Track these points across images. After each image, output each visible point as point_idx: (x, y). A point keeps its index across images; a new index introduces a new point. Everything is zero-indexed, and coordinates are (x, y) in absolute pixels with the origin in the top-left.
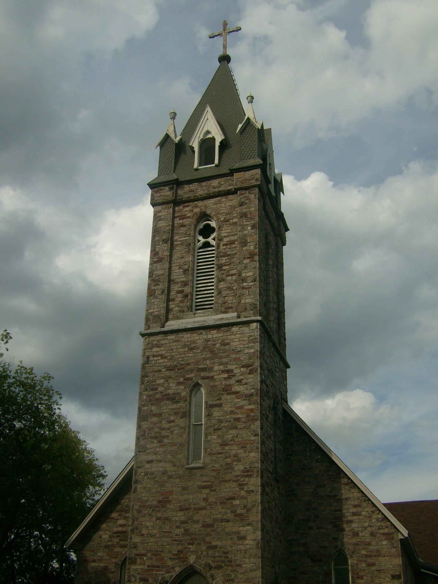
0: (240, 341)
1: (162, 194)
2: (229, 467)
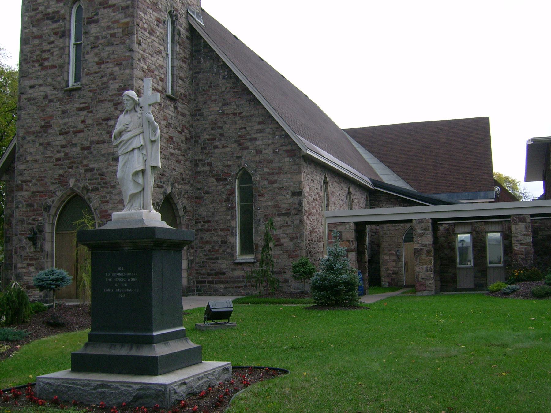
2: (105, 86)
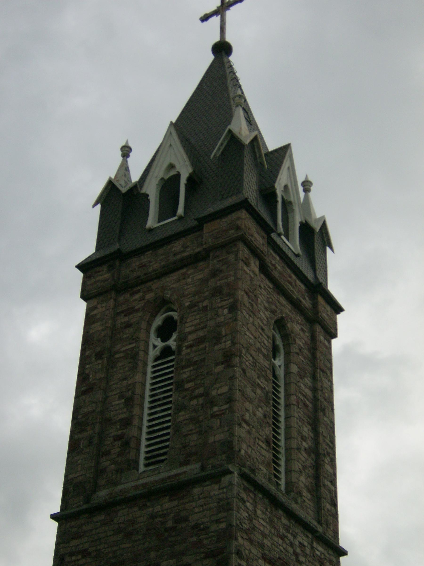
0: (204, 510)
1: (98, 279)
